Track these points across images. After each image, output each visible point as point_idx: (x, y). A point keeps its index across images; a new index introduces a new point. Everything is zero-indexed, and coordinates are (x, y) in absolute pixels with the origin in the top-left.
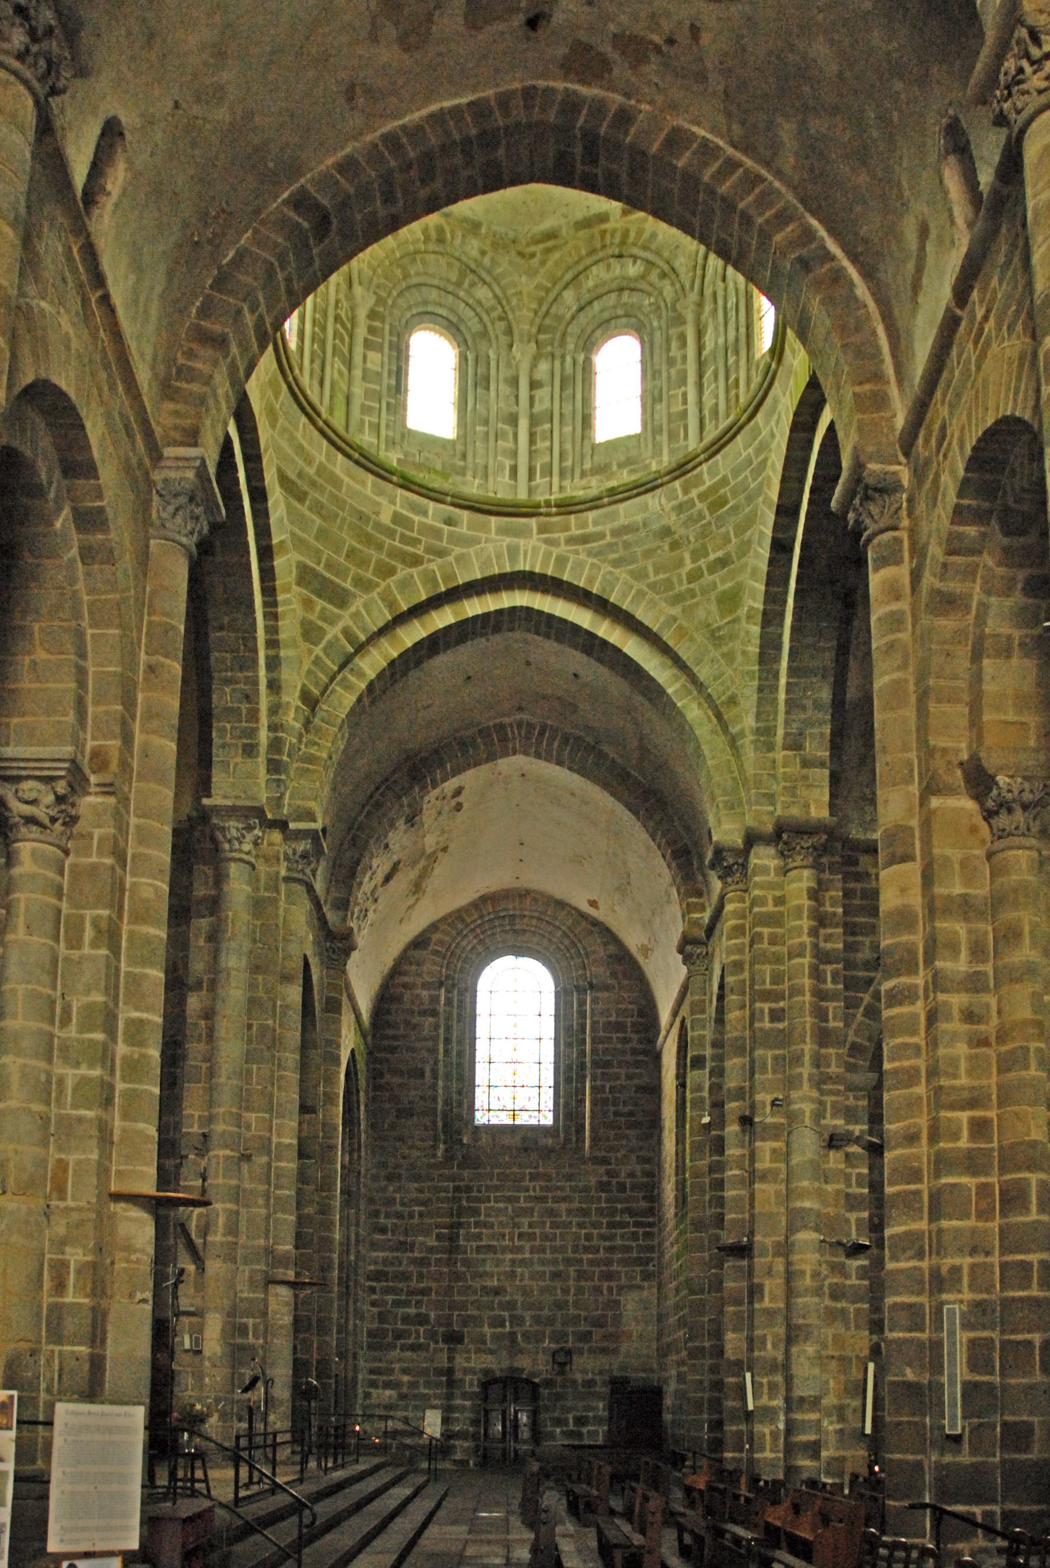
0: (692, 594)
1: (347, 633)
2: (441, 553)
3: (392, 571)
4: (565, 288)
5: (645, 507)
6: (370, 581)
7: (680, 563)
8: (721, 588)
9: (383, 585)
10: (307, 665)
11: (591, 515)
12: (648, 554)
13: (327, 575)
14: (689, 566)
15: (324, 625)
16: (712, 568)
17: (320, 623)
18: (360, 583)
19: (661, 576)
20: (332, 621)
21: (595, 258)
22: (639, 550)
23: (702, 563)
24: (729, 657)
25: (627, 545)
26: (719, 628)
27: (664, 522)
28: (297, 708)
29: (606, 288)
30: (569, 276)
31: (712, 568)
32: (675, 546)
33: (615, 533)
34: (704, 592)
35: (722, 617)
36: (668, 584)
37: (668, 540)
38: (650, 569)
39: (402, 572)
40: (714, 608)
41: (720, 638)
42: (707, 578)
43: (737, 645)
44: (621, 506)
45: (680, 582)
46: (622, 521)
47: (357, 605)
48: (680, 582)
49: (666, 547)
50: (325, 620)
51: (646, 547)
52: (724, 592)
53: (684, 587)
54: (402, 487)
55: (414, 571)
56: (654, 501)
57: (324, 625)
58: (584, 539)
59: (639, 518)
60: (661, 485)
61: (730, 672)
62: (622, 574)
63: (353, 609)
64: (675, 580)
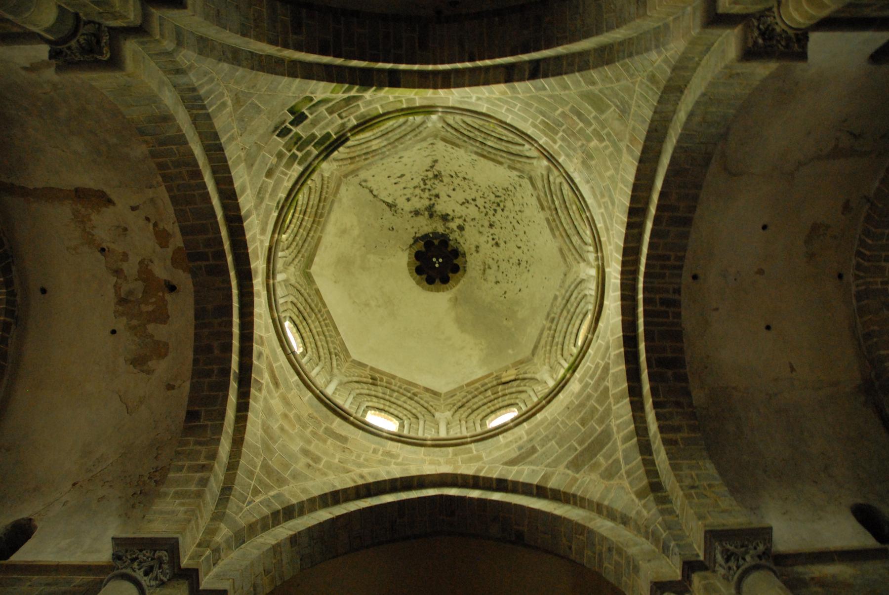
0: (609, 135)
1: (626, 440)
2: (608, 348)
3: (606, 389)
6: (605, 409)
8: (594, 113)
9: (611, 400)
10: (626, 484)
13: (586, 444)
14: (594, 143)
15: (614, 457)
16: (589, 124)
17: (610, 461)
18: (601, 421)
19: (609, 164)
20: (614, 450)
21: (559, 225)
26: (617, 106)
27: (579, 166)
28: (644, 506)
31: (589, 124)
32: (591, 157)
38: (608, 174)
39: (609, 383)
41: (622, 103)
45: (606, 147)
47: (614, 423)
48: (606, 147)
50: (610, 457)
53: (607, 143)
54: (574, 371)
55: (611, 371)
57: (614, 457)
62: (617, 197)
63: (615, 429)
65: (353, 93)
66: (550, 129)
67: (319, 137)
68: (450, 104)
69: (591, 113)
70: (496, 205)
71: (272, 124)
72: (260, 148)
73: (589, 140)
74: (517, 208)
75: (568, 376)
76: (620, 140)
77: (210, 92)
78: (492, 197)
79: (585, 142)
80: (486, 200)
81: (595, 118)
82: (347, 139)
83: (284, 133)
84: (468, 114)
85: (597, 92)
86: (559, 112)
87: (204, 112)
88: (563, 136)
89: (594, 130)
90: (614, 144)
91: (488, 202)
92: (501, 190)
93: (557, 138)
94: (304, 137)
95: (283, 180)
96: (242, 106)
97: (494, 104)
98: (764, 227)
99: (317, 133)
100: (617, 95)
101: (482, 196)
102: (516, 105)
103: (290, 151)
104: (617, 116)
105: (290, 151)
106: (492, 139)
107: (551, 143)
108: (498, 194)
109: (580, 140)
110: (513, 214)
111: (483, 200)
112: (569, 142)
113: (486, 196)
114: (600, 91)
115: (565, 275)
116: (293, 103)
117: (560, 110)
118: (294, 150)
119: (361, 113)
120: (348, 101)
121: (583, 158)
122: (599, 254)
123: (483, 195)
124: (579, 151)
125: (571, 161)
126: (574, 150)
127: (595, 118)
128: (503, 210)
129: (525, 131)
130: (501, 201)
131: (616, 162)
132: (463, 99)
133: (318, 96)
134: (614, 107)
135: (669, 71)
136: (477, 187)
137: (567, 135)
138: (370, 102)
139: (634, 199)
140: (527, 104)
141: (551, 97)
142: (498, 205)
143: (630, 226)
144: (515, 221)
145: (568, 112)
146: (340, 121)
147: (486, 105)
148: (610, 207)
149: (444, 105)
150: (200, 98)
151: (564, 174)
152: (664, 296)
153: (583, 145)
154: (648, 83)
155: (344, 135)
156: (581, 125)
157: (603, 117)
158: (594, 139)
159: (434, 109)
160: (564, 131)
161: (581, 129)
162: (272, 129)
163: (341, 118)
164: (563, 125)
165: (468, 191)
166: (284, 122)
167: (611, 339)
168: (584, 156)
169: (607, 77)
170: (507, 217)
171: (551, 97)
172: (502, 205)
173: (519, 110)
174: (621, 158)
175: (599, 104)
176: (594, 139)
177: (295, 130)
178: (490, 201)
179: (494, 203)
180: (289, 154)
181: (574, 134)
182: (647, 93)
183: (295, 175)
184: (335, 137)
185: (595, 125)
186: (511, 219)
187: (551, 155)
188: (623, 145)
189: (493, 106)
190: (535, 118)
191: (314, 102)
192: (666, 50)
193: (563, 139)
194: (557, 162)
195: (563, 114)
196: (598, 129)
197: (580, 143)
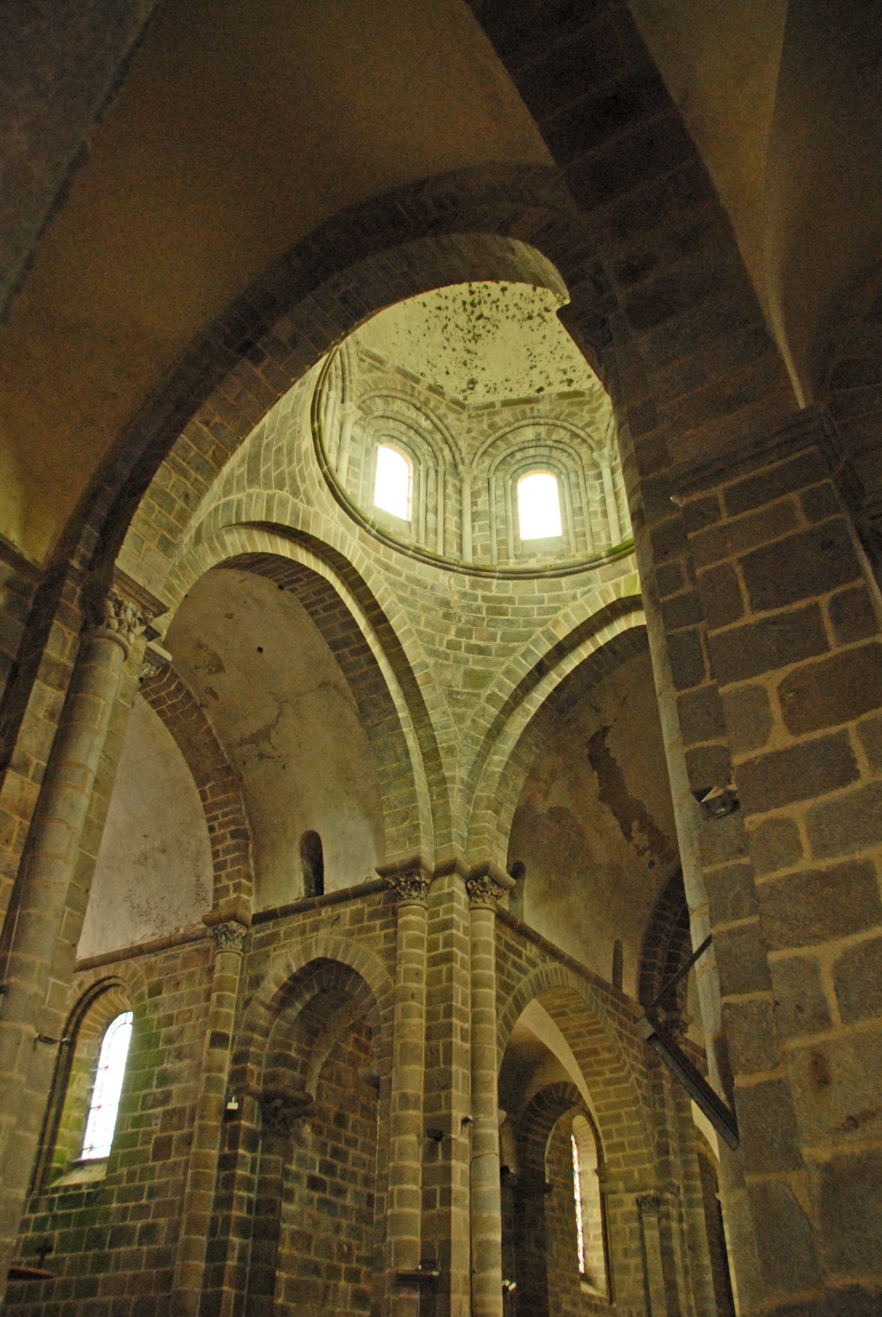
0: (447, 657)
4: (379, 396)
5: (437, 578)
7: (446, 631)
8: (471, 666)
11: (395, 555)
12: (427, 609)
14: (452, 636)
16: (470, 649)
19: (428, 630)
21: (405, 397)
22: (421, 602)
23: (464, 641)
24: (460, 719)
25: (413, 593)
26: (458, 693)
27: (448, 596)
29: (403, 419)
30: (385, 392)
31: (470, 649)
32: (447, 616)
33: (408, 578)
34: (456, 661)
35: (465, 686)
36: (431, 640)
37: (444, 609)
38: (423, 620)
39: (285, 493)
40: (459, 676)
41: (457, 700)
42: (462, 654)
43: (470, 713)
44: (419, 565)
45: (441, 644)
46: (416, 574)
48: (441, 644)
49: (441, 614)
51: (426, 603)
52: (473, 671)
53: (443, 648)
56: (444, 578)
58: (387, 568)
59: (430, 581)
64: (437, 639)
66: (496, 609)
68: (597, 571)
69: (474, 663)
70: (476, 301)
73: (460, 633)
74: (451, 326)
75: (316, 425)
76: (435, 664)
78: (485, 310)
79: (460, 625)
80: (489, 300)
81: (467, 661)
84: (576, 569)
85: (481, 691)
88: (481, 613)
89: (460, 648)
91: (486, 298)
92: (482, 332)
93: (484, 606)
97: (557, 599)
98: (260, 650)
100: (466, 705)
101: (498, 303)
102: (539, 614)
104: (453, 684)
106: (531, 445)
107: (487, 594)
108: (481, 322)
109: (465, 624)
110: (450, 313)
111: (494, 297)
112: (472, 611)
113: (494, 306)
114: (478, 696)
115: (358, 343)
117: (498, 641)
121: (452, 608)
122: (374, 532)
123: (497, 307)
124: (458, 611)
125: (458, 592)
126: (463, 608)
127: (467, 661)
128: (464, 303)
129: (515, 582)
130: (473, 312)
131: (425, 639)
132: (589, 587)
134: (460, 689)
135: (447, 774)
136: (510, 314)
137: (478, 617)
140: (528, 624)
141: (514, 650)
142: (473, 304)
143: (375, 605)
144: (443, 306)
145: (491, 644)
147: (564, 592)
148: (400, 593)
151: (455, 568)
152: (302, 583)
153: (460, 621)
154: (452, 743)
156: (473, 641)
157: (462, 669)
158: (455, 638)
159: (611, 557)
160: (483, 619)
161: (470, 637)
164: (488, 626)
165: (517, 300)
167: (312, 510)
168: (452, 611)
169: (483, 716)
170: (454, 300)
171: (514, 650)
172: (468, 307)
173: (533, 609)
174: (425, 648)
176: (455, 638)
178: (485, 302)
179: (480, 303)
181: (474, 623)
182: (447, 733)
185: (462, 654)
186: (449, 303)
188: (431, 661)
189: (558, 596)
190: (516, 612)
192: (460, 790)
193: (478, 610)
194: (469, 574)
195: (492, 637)
196: (457, 652)
197: (463, 620)
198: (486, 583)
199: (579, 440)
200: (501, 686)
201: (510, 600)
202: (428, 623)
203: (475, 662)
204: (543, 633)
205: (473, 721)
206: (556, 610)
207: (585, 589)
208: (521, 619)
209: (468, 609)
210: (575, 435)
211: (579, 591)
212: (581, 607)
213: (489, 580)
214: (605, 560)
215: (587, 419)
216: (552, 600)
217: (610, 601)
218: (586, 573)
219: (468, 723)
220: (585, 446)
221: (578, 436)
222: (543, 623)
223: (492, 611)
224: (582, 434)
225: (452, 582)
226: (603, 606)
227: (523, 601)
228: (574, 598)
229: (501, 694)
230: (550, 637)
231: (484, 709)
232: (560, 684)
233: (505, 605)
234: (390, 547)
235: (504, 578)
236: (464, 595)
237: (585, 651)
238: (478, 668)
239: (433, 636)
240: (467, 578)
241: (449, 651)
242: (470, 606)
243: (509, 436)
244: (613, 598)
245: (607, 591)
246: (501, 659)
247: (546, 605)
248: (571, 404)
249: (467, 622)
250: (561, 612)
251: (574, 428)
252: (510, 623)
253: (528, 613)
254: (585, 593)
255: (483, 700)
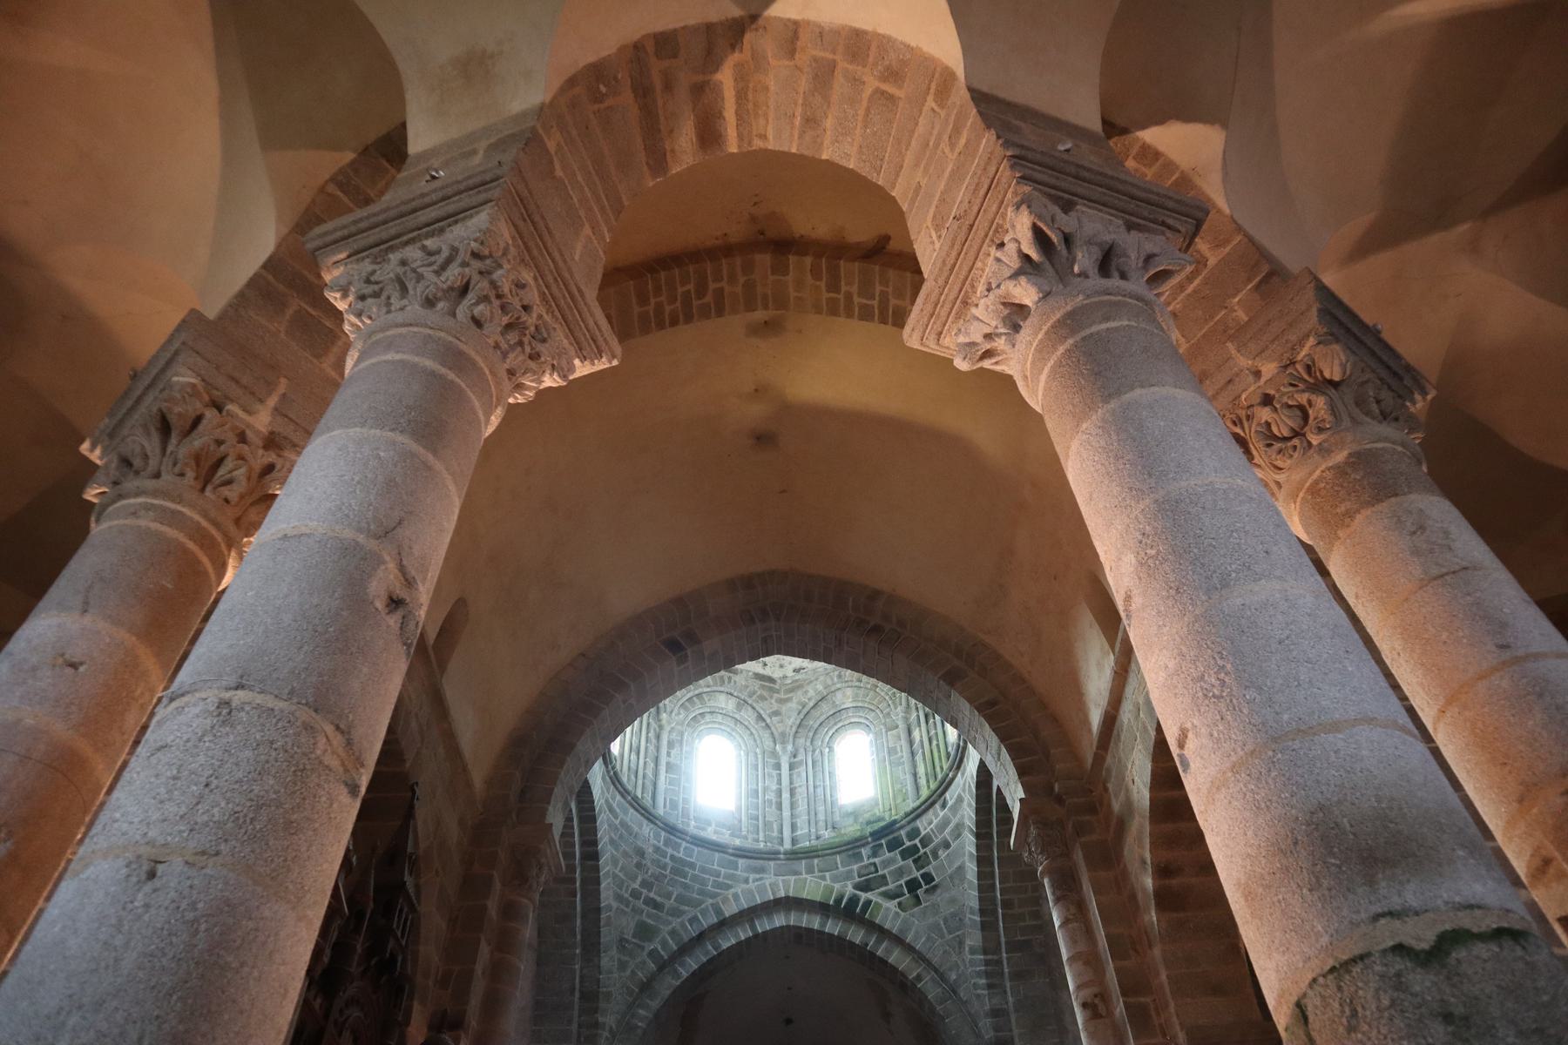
5: (640, 826)
7: (634, 879)
8: (644, 918)
11: (618, 797)
12: (626, 854)
14: (636, 886)
19: (621, 875)
24: (622, 966)
25: (621, 837)
26: (627, 941)
32: (639, 866)
33: (623, 824)
40: (632, 925)
42: (640, 904)
48: (626, 891)
53: (626, 895)
60: (656, 824)
61: (616, 975)
64: (626, 884)
65: (864, 896)
67: (897, 851)
68: (772, 863)
71: (937, 897)
72: (951, 877)
73: (644, 884)
77: (979, 974)
82: (872, 834)
83: (928, 878)
85: (646, 944)
86: (674, 897)
87: (990, 957)
90: (619, 898)
94: (911, 860)
95: (936, 826)
96: (958, 936)
97: (731, 877)
99: (899, 857)
102: (713, 886)
103: (925, 853)
105: (925, 853)
112: (659, 867)
114: (643, 948)
116: (916, 909)
118: (922, 851)
119: (856, 863)
120: (865, 887)
124: (649, 864)
125: (654, 845)
126: (653, 861)
133: (892, 905)
134: (629, 938)
135: (601, 1019)
138: (848, 876)
139: (597, 869)
140: (701, 892)
146: (876, 860)
147: (739, 873)
149: (779, 862)
150: (987, 974)
153: (647, 872)
154: (609, 989)
155: (874, 840)
156: (652, 895)
161: (650, 891)
162: (939, 891)
163: (875, 864)
164: (668, 884)
166: (927, 891)
168: (644, 862)
175: (644, 932)
177: (917, 874)
180: (927, 850)
183: (925, 819)
184: (883, 841)
185: (640, 904)
187: (671, 833)
188: (615, 904)
189: (733, 874)
190: (695, 878)
191: (898, 900)
193: (664, 867)
198: (676, 843)
199: (764, 724)
200: (664, 944)
201: (692, 866)
202: (622, 869)
203: (649, 916)
204: (712, 905)
205: (632, 971)
206: (729, 887)
207: (758, 876)
208: (697, 886)
209: (656, 863)
210: (760, 718)
211: (752, 876)
212: (750, 892)
213: (680, 841)
214: (782, 856)
215: (775, 706)
216: (727, 876)
217: (778, 896)
218: (761, 862)
219: (628, 972)
220: (768, 731)
221: (764, 720)
222: (714, 896)
223: (675, 871)
224: (768, 721)
225: (651, 834)
226: (772, 898)
227: (703, 870)
228: (746, 881)
229: (663, 953)
230: (718, 911)
231: (644, 963)
232: (714, 956)
233: (687, 869)
234: (617, 789)
235: (691, 843)
236: (657, 849)
237: (744, 933)
238: (649, 921)
239: (623, 882)
240: (663, 834)
241: (630, 899)
242: (659, 861)
243: (704, 695)
244: (782, 894)
245: (778, 886)
246: (670, 918)
247: (721, 880)
248: (763, 687)
249: (652, 875)
250: (732, 891)
251: (762, 712)
252: (686, 886)
253: (703, 882)
254: (757, 880)
255: (645, 953)
